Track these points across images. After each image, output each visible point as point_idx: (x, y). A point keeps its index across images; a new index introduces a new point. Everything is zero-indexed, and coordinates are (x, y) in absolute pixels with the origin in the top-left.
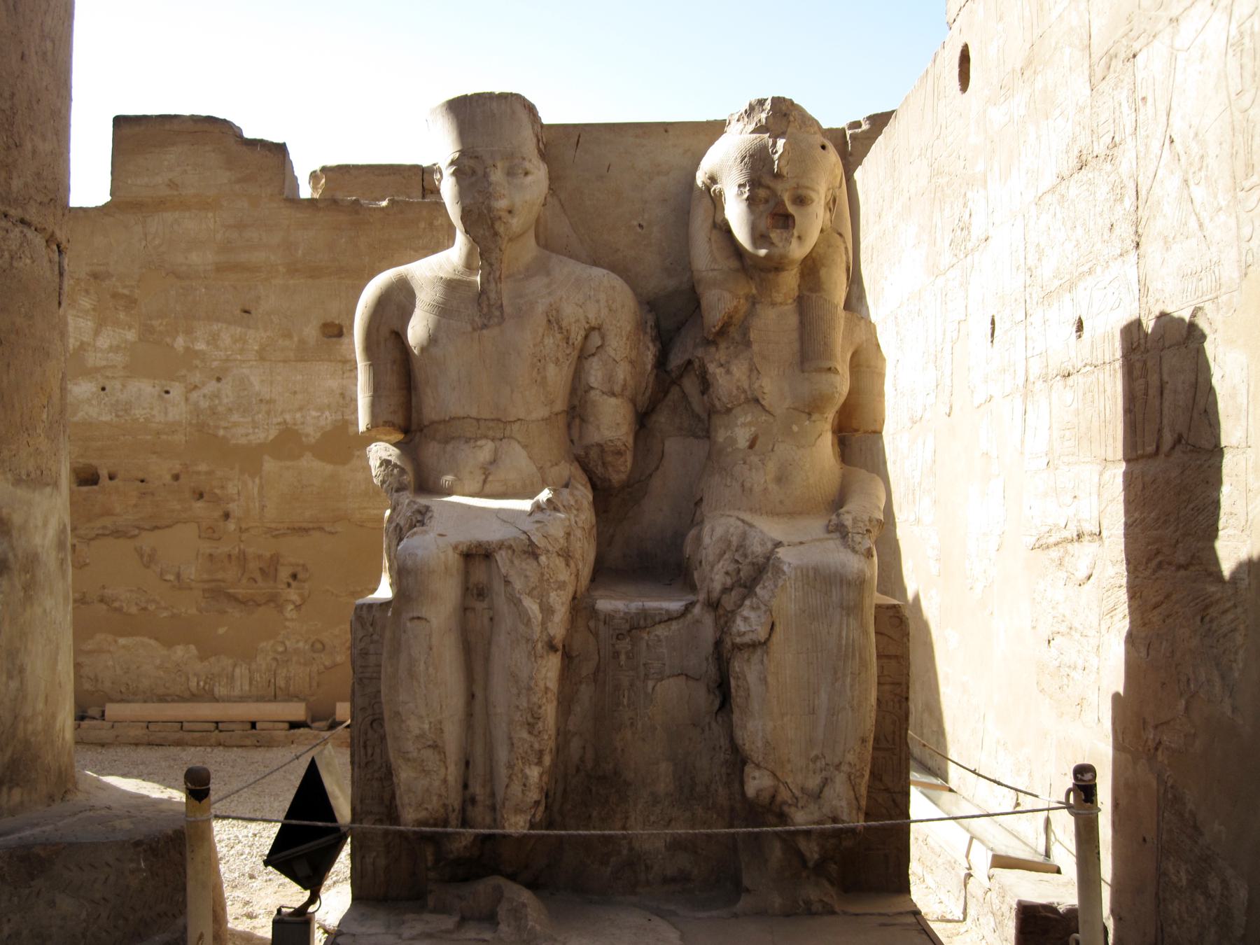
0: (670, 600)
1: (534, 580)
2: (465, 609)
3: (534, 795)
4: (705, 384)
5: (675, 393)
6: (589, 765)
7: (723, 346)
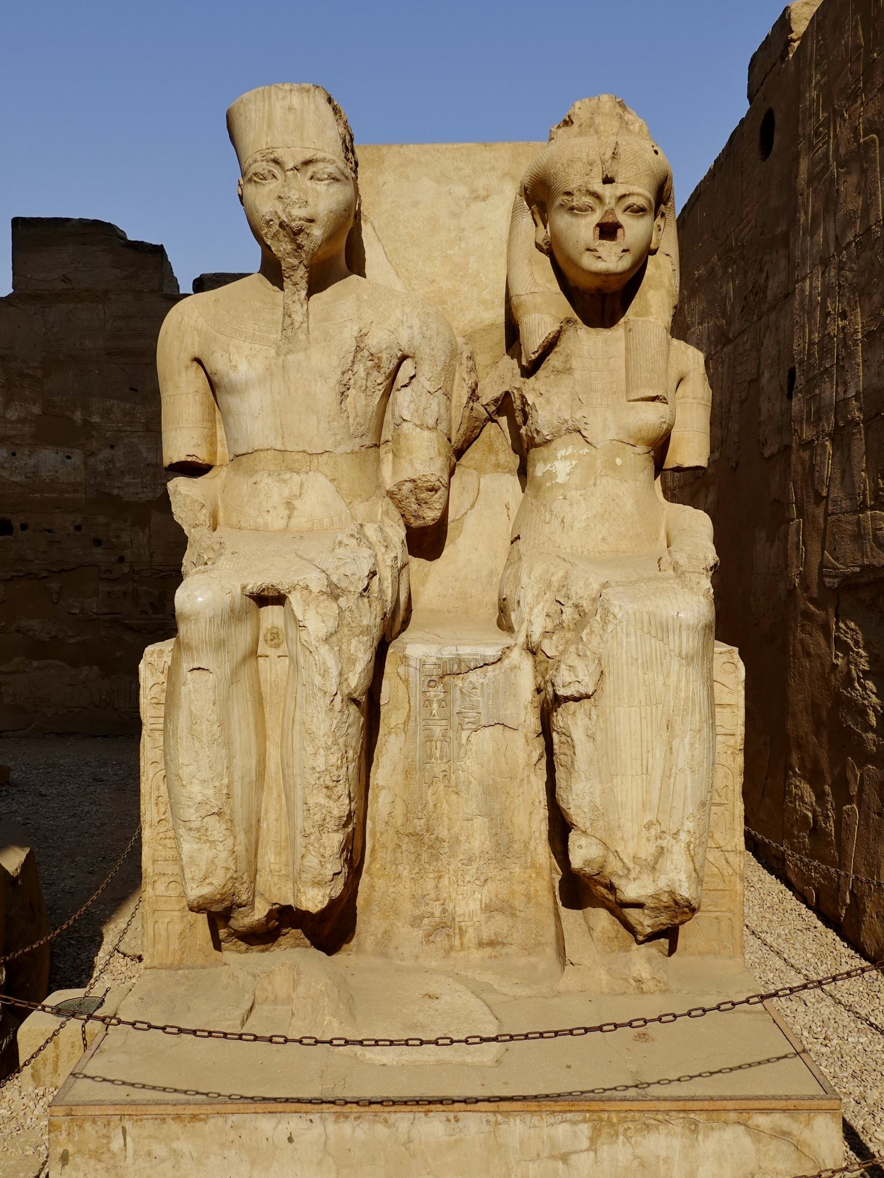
0: (488, 645)
1: (332, 624)
6: (399, 820)
7: (541, 373)
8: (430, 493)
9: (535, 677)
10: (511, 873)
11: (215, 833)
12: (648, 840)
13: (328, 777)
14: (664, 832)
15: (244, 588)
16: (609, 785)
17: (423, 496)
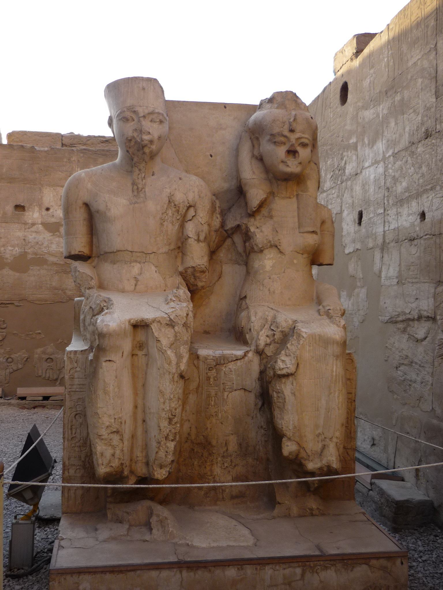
1: (172, 339)
3: (170, 458)
4: (247, 236)
5: (229, 242)
6: (193, 437)
7: (258, 218)
8: (202, 274)
10: (247, 462)
12: (318, 442)
14: (326, 438)
15: (129, 321)
17: (198, 275)
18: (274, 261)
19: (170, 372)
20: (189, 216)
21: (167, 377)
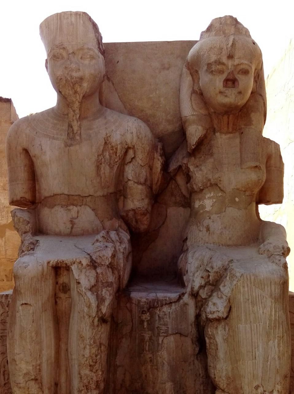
0: (171, 292)
1: (93, 281)
2: (55, 297)
4: (189, 178)
9: (196, 310)
11: (33, 389)
13: (91, 360)
15: (49, 263)
16: (236, 365)
17: (139, 217)
18: (214, 200)
19: (90, 316)
20: (128, 158)
21: (88, 321)
